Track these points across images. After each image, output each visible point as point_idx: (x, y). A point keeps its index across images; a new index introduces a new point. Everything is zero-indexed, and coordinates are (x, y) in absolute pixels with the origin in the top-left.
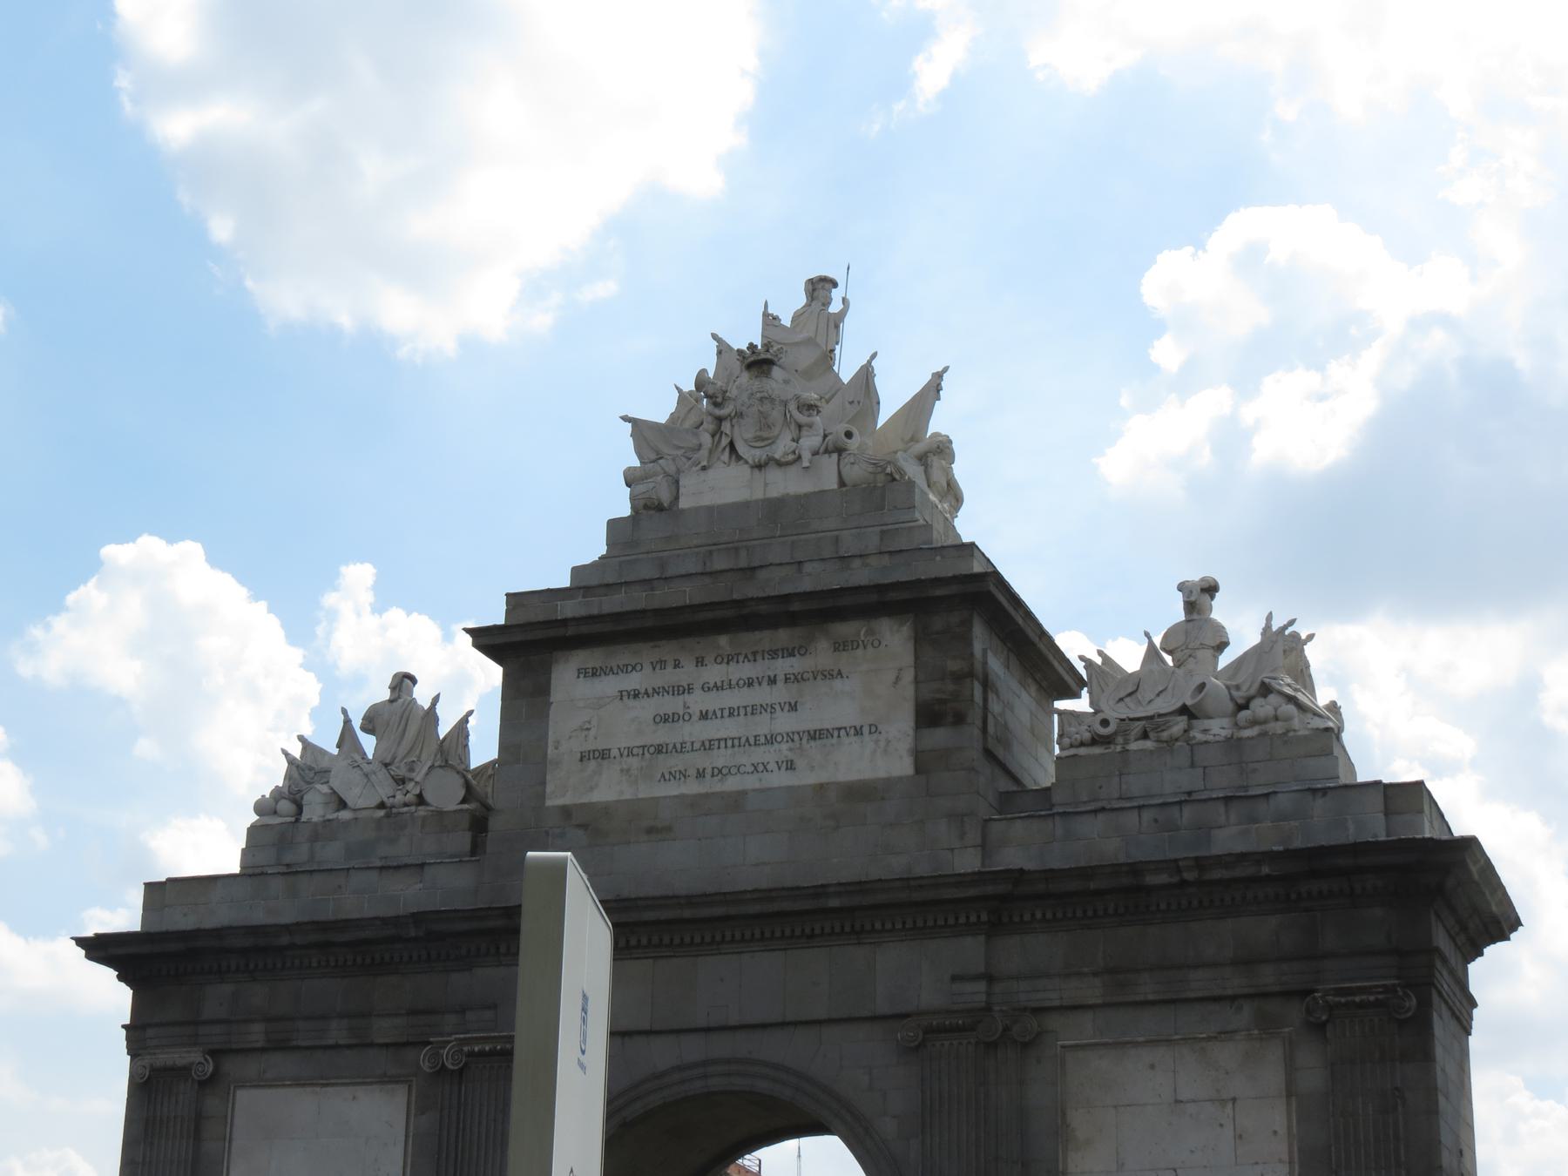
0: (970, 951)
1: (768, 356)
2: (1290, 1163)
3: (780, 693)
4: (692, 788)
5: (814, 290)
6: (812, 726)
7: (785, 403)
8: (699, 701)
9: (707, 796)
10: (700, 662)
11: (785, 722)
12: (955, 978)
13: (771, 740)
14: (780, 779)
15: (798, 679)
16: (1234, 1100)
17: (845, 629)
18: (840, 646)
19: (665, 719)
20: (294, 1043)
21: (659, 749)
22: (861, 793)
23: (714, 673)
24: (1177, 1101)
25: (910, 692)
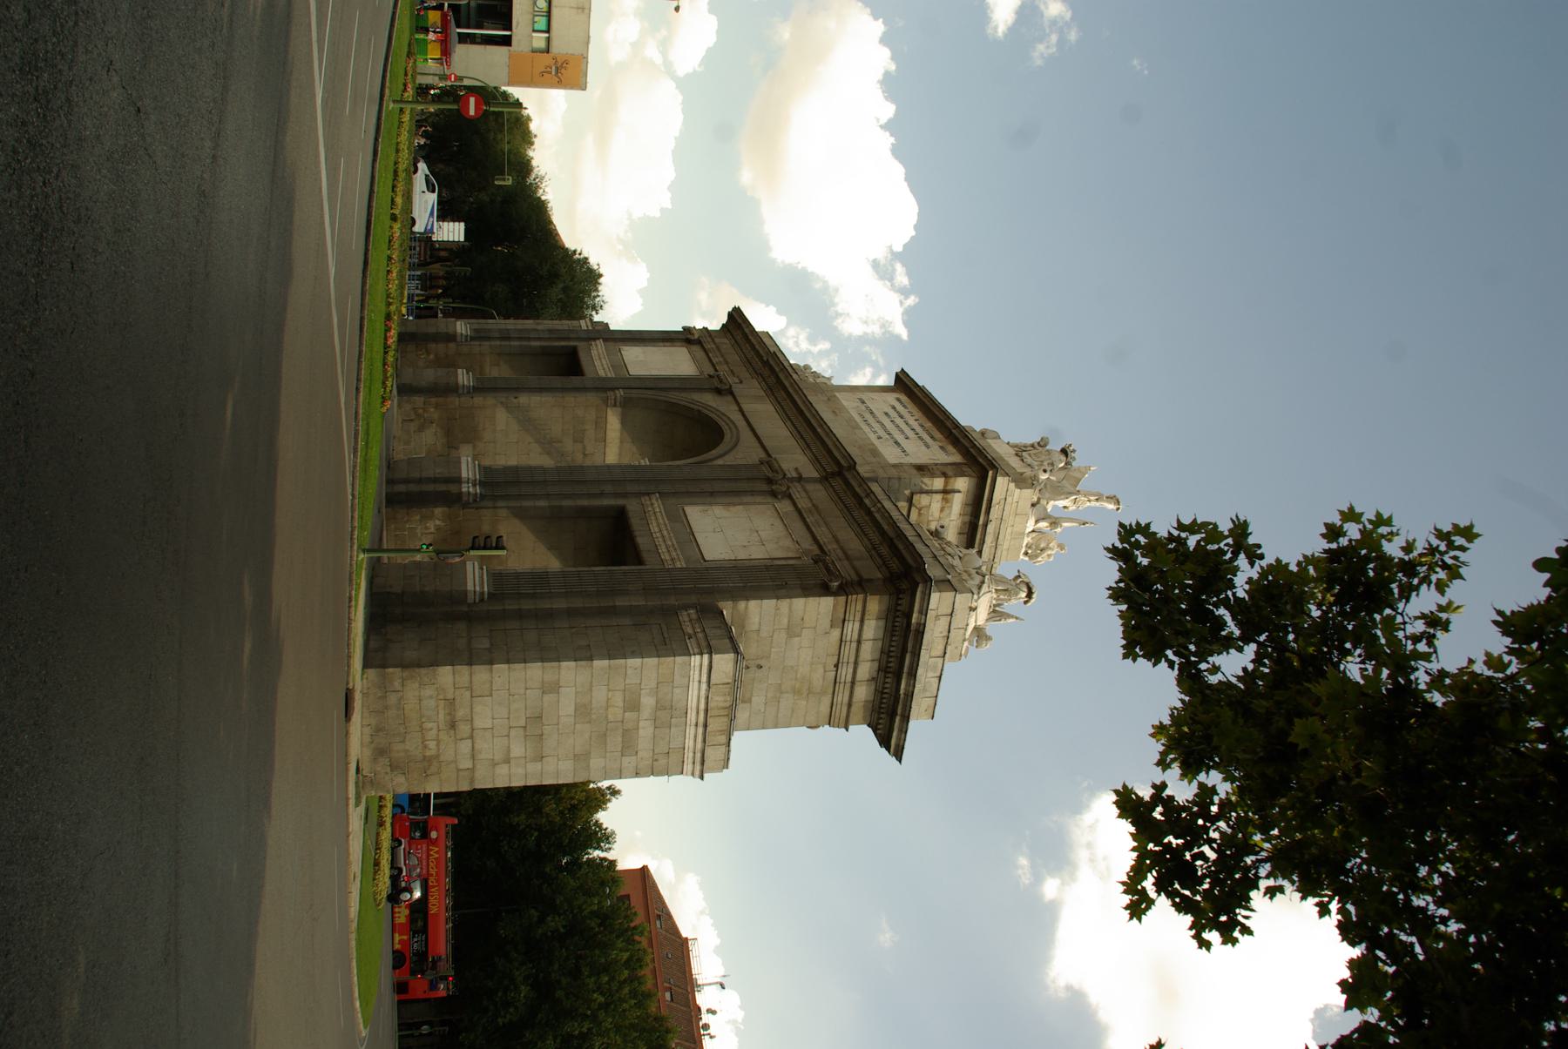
0: (810, 472)
1: (1069, 453)
2: (735, 560)
3: (910, 434)
4: (858, 419)
5: (1112, 498)
6: (899, 441)
7: (1050, 459)
8: (899, 421)
9: (855, 422)
10: (916, 420)
11: (900, 438)
12: (796, 469)
13: (889, 434)
14: (873, 437)
15: (921, 438)
16: (763, 545)
17: (950, 448)
18: (942, 448)
19: (886, 414)
20: (710, 355)
21: (872, 413)
22: (875, 452)
23: (912, 422)
24: (757, 532)
25: (929, 462)
